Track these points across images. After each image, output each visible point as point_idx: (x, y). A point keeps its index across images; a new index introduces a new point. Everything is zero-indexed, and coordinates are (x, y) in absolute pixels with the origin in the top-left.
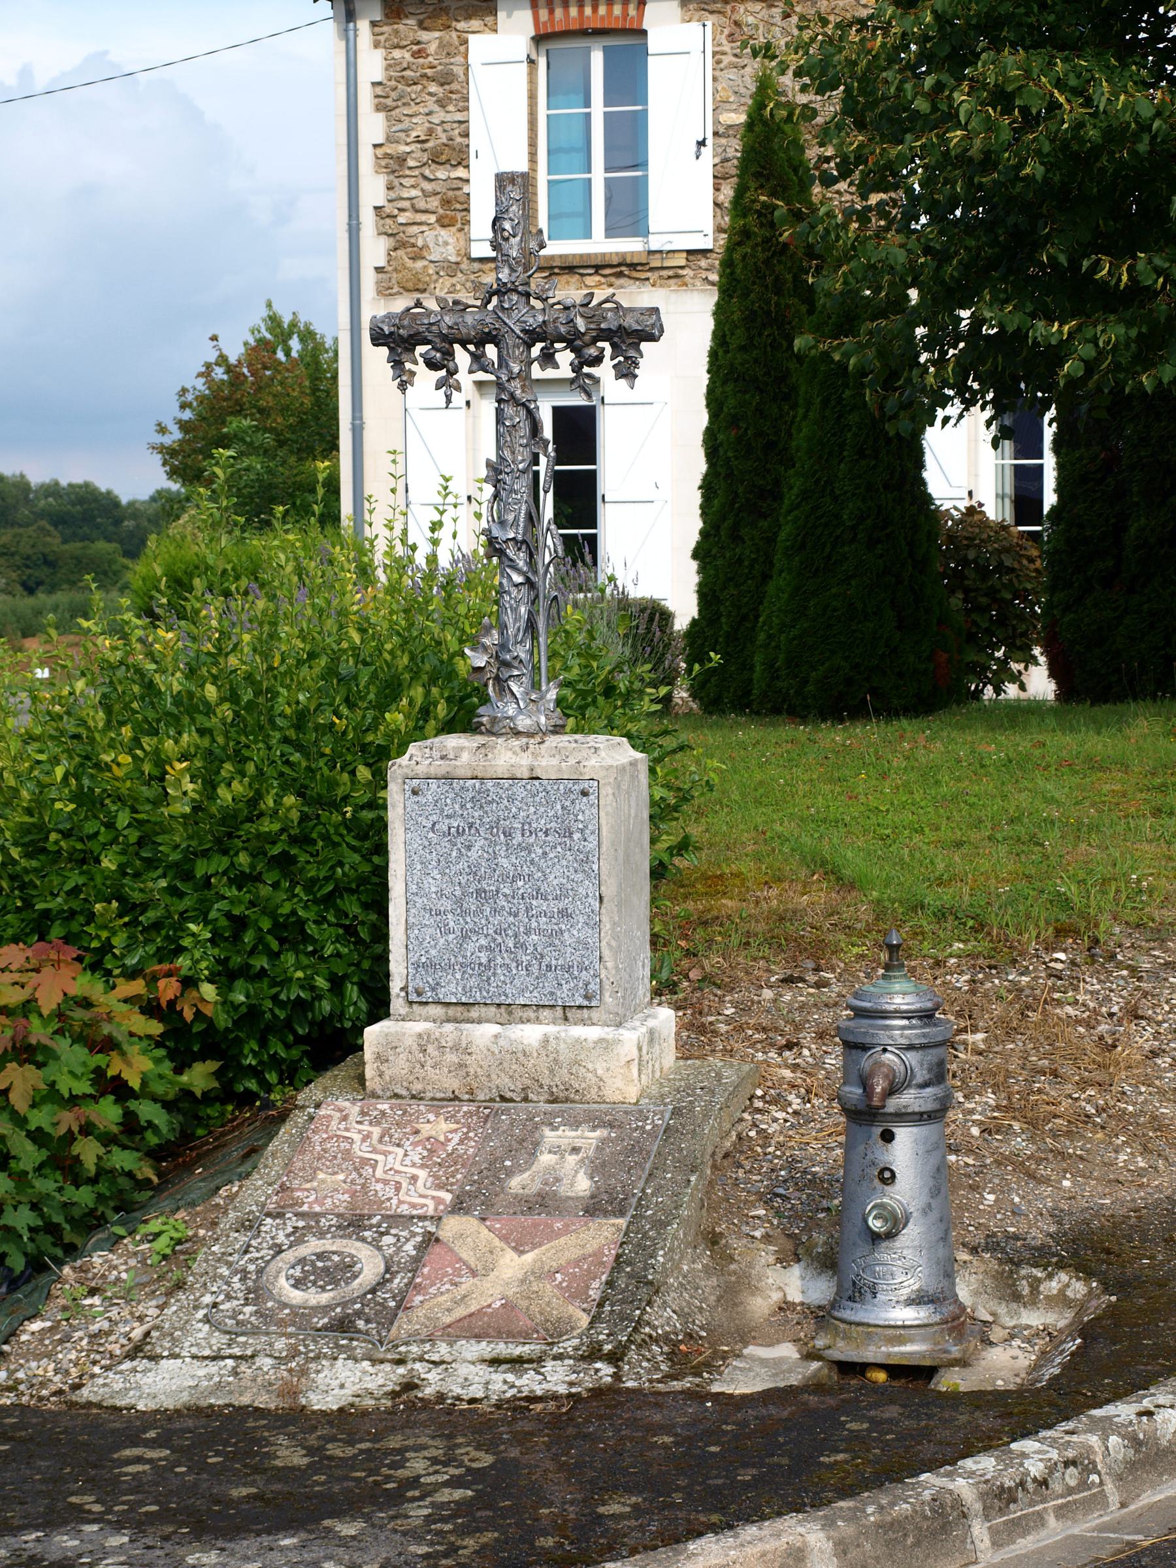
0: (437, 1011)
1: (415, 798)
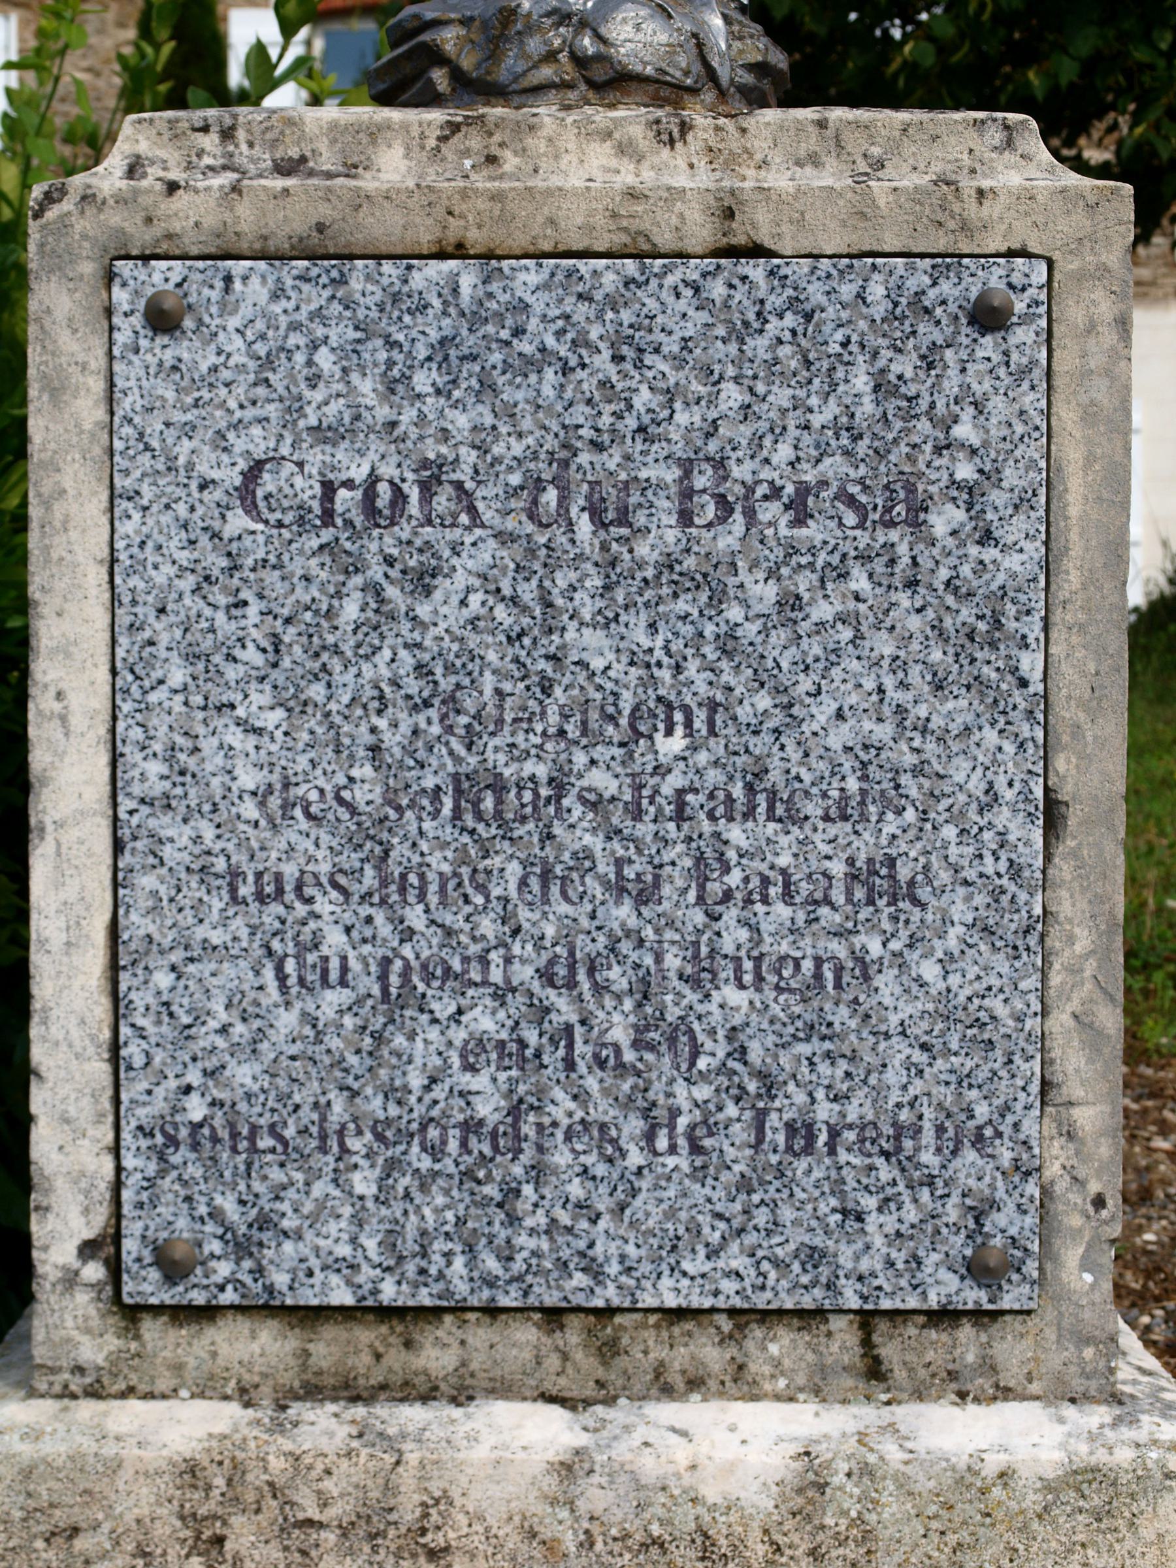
0: (260, 1346)
1: (165, 350)
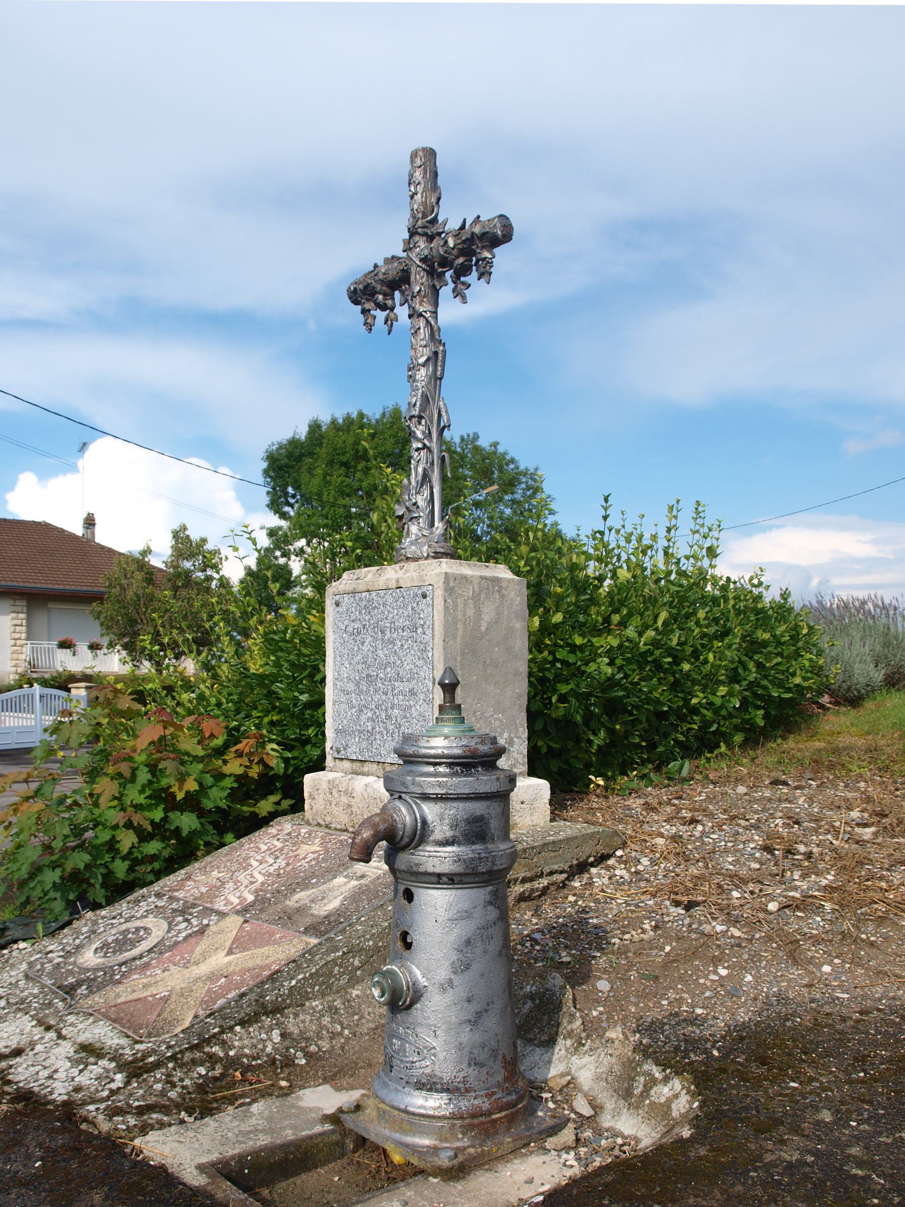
0: (346, 765)
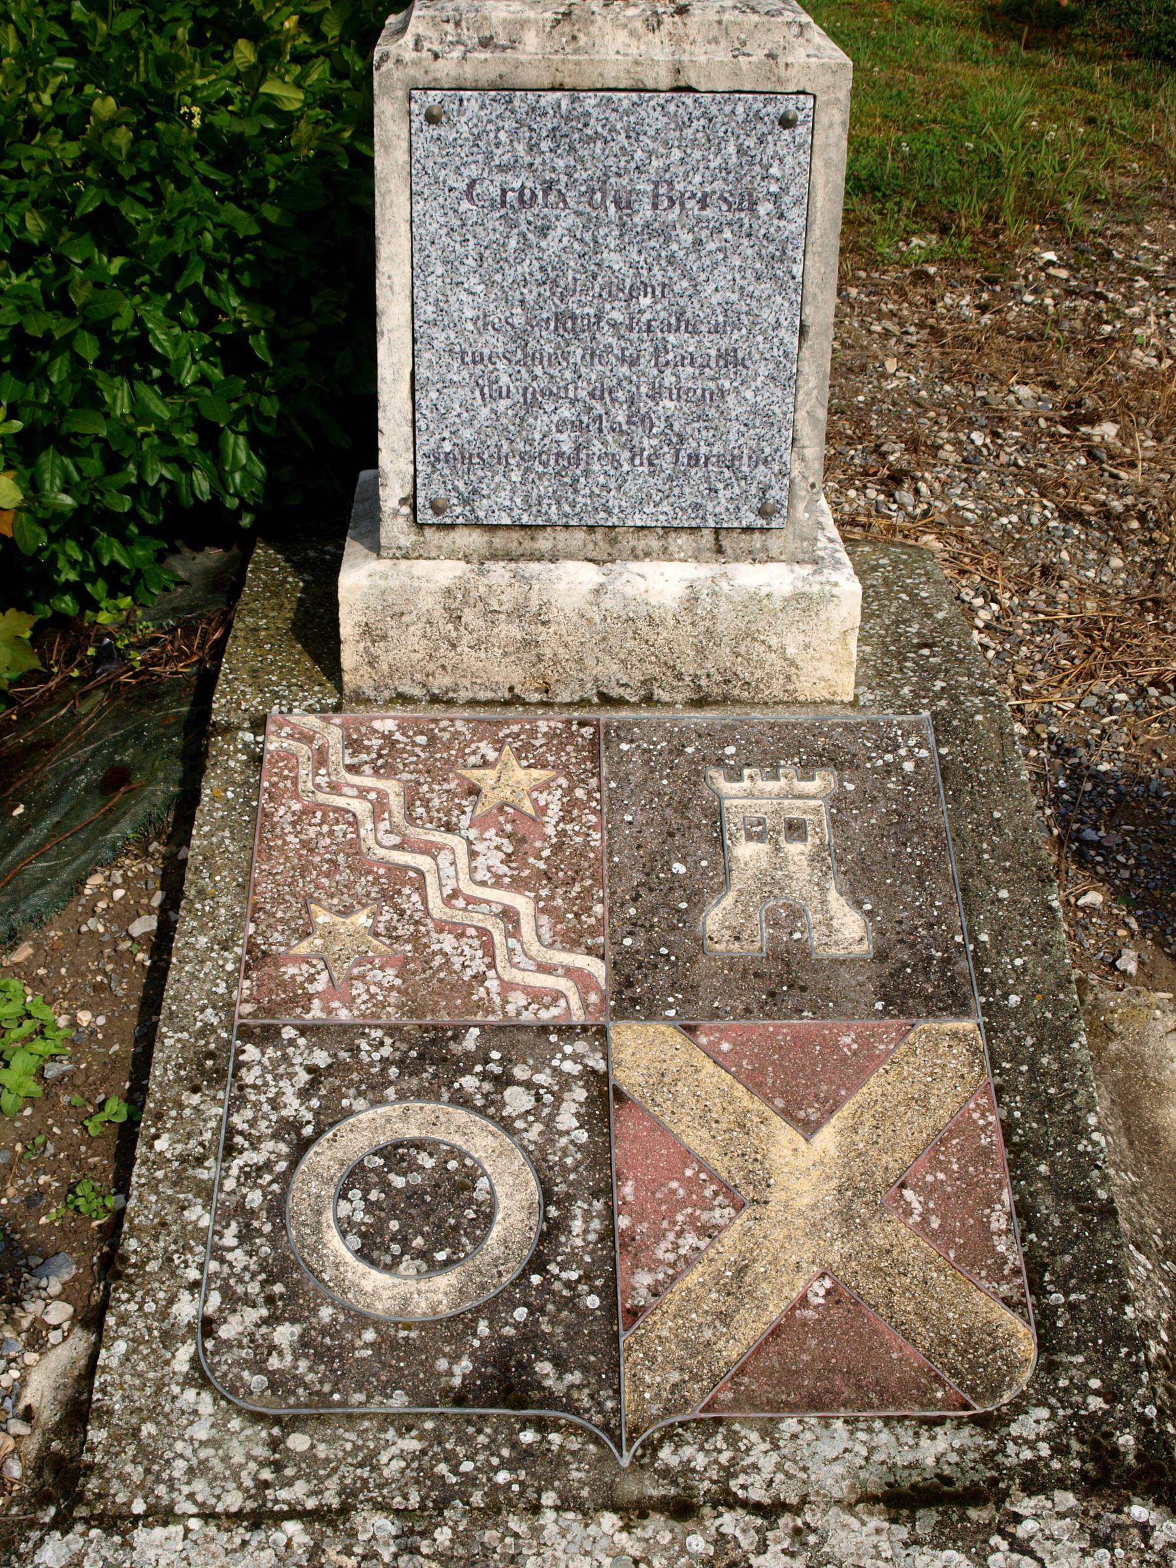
0: (474, 540)
1: (433, 131)
